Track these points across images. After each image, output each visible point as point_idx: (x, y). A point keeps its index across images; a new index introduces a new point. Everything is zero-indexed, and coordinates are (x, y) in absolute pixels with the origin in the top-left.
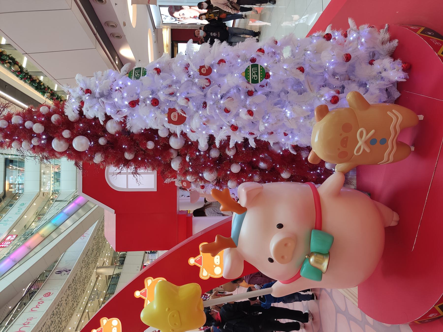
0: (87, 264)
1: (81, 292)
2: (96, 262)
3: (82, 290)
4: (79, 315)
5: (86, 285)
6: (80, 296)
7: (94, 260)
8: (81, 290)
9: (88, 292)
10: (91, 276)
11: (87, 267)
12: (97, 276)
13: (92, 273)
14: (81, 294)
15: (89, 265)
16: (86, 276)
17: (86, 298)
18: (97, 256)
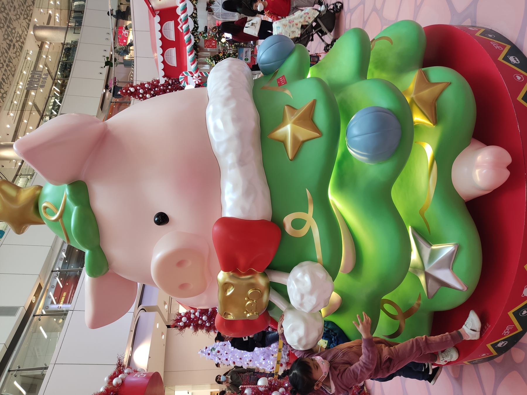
0: (5, 22)
1: (4, 74)
2: (28, 17)
3: (8, 71)
4: (12, 114)
5: (14, 61)
6: (4, 81)
7: (23, 13)
8: (4, 72)
9: (25, 72)
10: (23, 43)
11: (6, 27)
12: (40, 42)
13: (25, 39)
14: (8, 78)
15: (10, 22)
16: (10, 45)
17: (21, 83)
18: (27, 4)
